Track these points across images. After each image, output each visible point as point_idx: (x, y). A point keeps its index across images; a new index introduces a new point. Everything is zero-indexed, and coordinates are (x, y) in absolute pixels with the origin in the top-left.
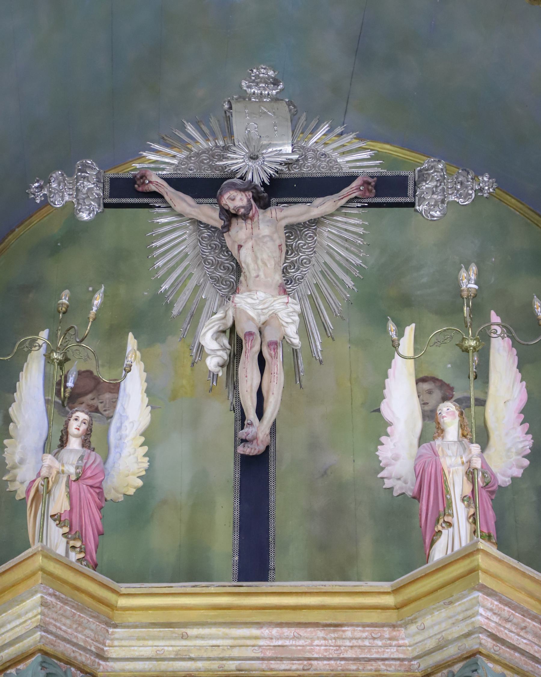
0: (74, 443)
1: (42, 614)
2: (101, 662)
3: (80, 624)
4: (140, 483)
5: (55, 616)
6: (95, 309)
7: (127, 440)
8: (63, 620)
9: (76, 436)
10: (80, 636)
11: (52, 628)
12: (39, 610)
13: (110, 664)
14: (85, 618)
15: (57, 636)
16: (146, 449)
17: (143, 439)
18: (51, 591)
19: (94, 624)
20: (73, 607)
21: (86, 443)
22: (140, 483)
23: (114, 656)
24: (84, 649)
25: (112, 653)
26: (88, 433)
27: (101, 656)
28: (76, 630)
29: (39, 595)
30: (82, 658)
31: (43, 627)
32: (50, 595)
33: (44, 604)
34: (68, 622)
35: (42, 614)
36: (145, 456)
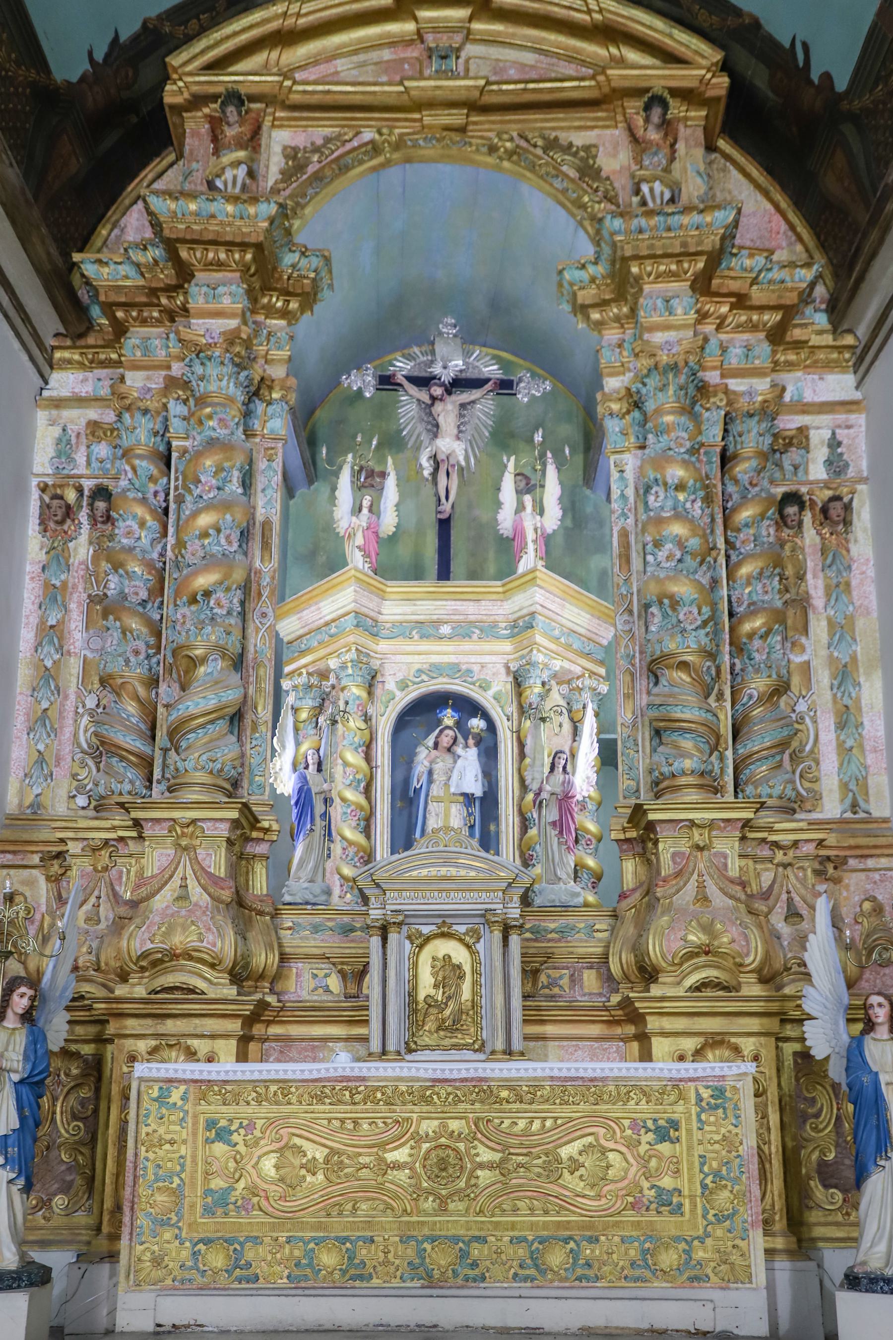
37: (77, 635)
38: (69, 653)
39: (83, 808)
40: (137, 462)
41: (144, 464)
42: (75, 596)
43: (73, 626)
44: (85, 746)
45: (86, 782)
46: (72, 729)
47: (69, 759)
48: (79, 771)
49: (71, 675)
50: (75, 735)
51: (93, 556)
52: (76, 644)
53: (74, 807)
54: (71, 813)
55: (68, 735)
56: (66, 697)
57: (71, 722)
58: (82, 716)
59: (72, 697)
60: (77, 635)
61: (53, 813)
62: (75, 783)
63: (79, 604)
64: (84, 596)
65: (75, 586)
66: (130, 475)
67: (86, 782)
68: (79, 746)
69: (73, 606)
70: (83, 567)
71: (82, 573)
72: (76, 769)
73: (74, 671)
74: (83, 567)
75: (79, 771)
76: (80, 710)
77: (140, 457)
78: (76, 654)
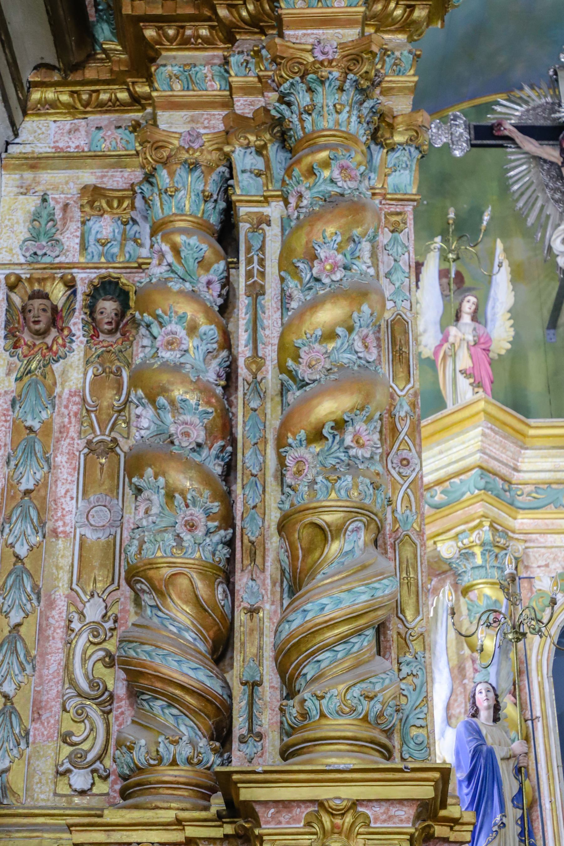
0: (466, 318)
1: (482, 441)
2: (516, 474)
3: (504, 448)
4: (509, 346)
5: (489, 442)
6: (485, 223)
7: (498, 316)
8: (495, 445)
9: (468, 314)
10: (504, 456)
11: (488, 451)
12: (480, 438)
13: (521, 474)
14: (509, 444)
15: (490, 456)
16: (512, 322)
17: (509, 315)
18: (489, 425)
19: (513, 448)
20: (501, 436)
21: (474, 318)
22: (509, 346)
23: (525, 469)
24: (506, 465)
25: (523, 466)
26: (476, 311)
27: (516, 469)
28: (502, 452)
29: (480, 429)
30: (504, 471)
31: (483, 451)
32: (488, 428)
33: (484, 435)
34: (497, 446)
35: (482, 441)
36: (512, 326)
37: (69, 505)
38: (55, 533)
39: (82, 793)
40: (180, 239)
41: (194, 241)
42: (65, 444)
43: (61, 490)
44: (84, 685)
45: (85, 746)
46: (61, 656)
47: (57, 708)
48: (74, 728)
49: (58, 568)
50: (68, 667)
51: (92, 383)
52: (67, 519)
53: (66, 791)
54: (63, 802)
55: (54, 667)
56: (51, 604)
57: (60, 645)
58: (79, 634)
59: (62, 603)
60: (69, 505)
61: (29, 802)
62: (67, 750)
63: (71, 455)
64: (80, 444)
65: (63, 429)
66: (170, 258)
67: (85, 746)
68: (73, 683)
69: (61, 459)
70: (77, 399)
71: (75, 408)
72: (67, 725)
73: (65, 562)
74: (77, 399)
75: (74, 728)
76: (76, 625)
77: (183, 231)
78: (66, 534)
